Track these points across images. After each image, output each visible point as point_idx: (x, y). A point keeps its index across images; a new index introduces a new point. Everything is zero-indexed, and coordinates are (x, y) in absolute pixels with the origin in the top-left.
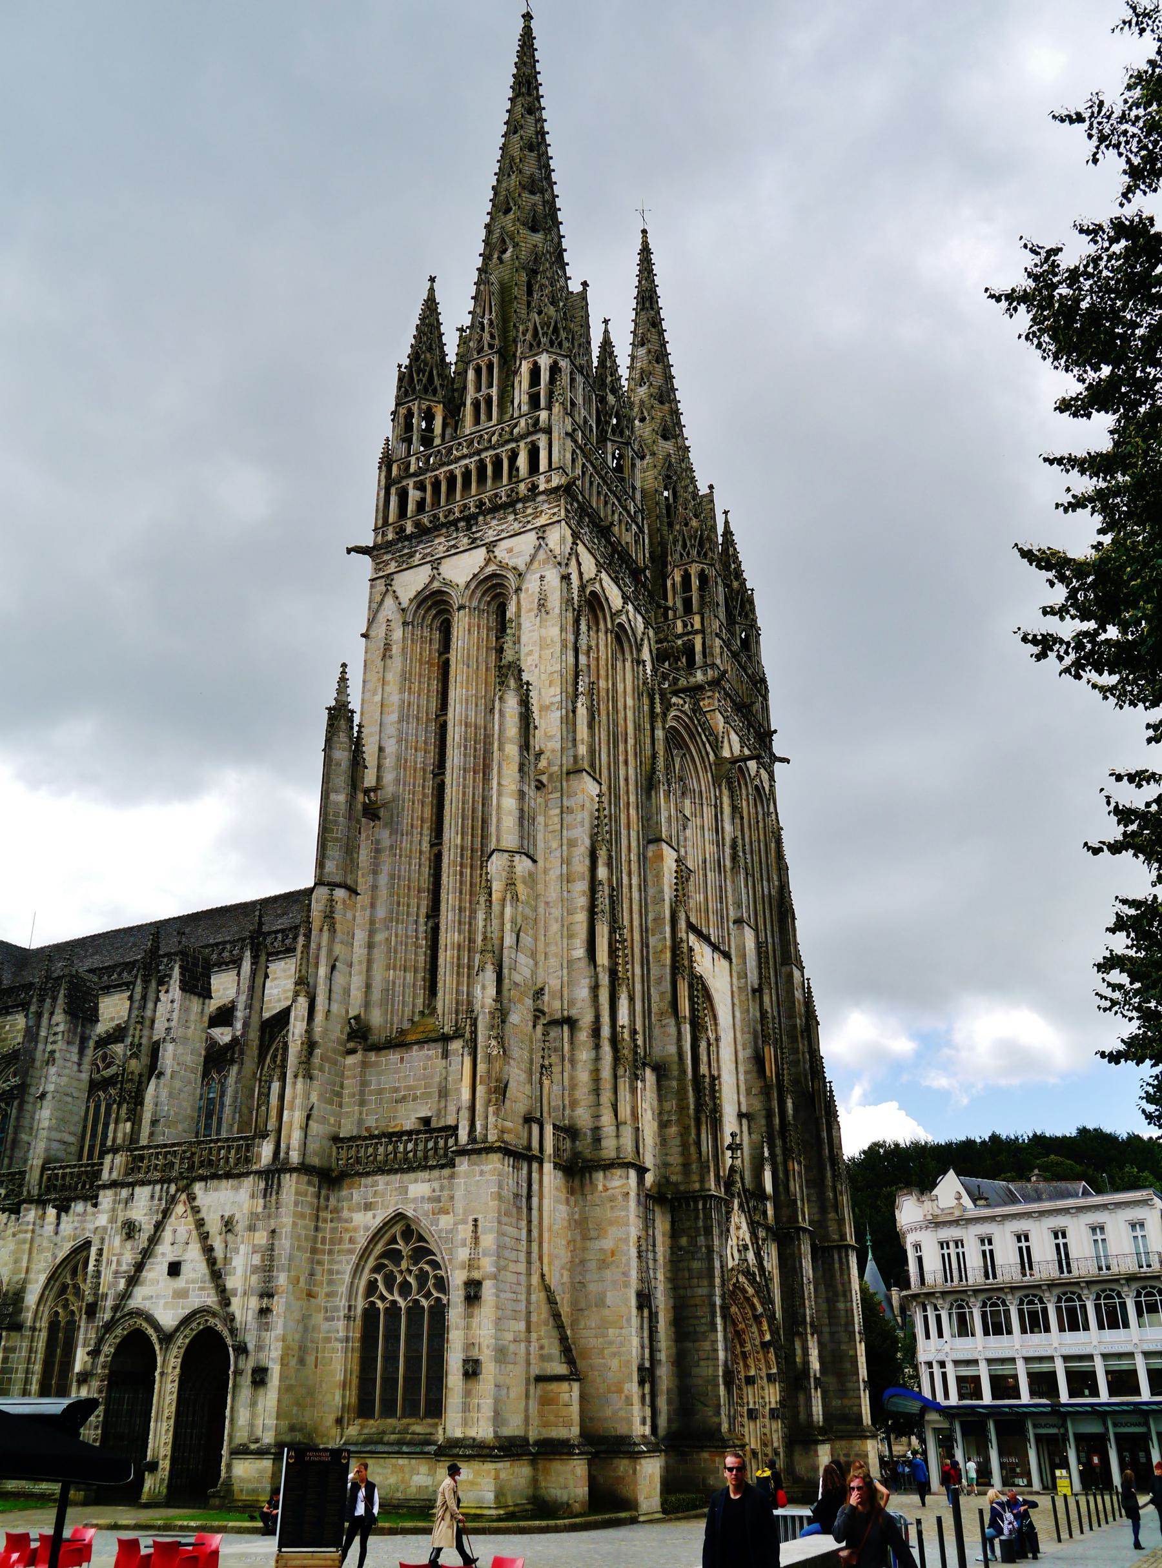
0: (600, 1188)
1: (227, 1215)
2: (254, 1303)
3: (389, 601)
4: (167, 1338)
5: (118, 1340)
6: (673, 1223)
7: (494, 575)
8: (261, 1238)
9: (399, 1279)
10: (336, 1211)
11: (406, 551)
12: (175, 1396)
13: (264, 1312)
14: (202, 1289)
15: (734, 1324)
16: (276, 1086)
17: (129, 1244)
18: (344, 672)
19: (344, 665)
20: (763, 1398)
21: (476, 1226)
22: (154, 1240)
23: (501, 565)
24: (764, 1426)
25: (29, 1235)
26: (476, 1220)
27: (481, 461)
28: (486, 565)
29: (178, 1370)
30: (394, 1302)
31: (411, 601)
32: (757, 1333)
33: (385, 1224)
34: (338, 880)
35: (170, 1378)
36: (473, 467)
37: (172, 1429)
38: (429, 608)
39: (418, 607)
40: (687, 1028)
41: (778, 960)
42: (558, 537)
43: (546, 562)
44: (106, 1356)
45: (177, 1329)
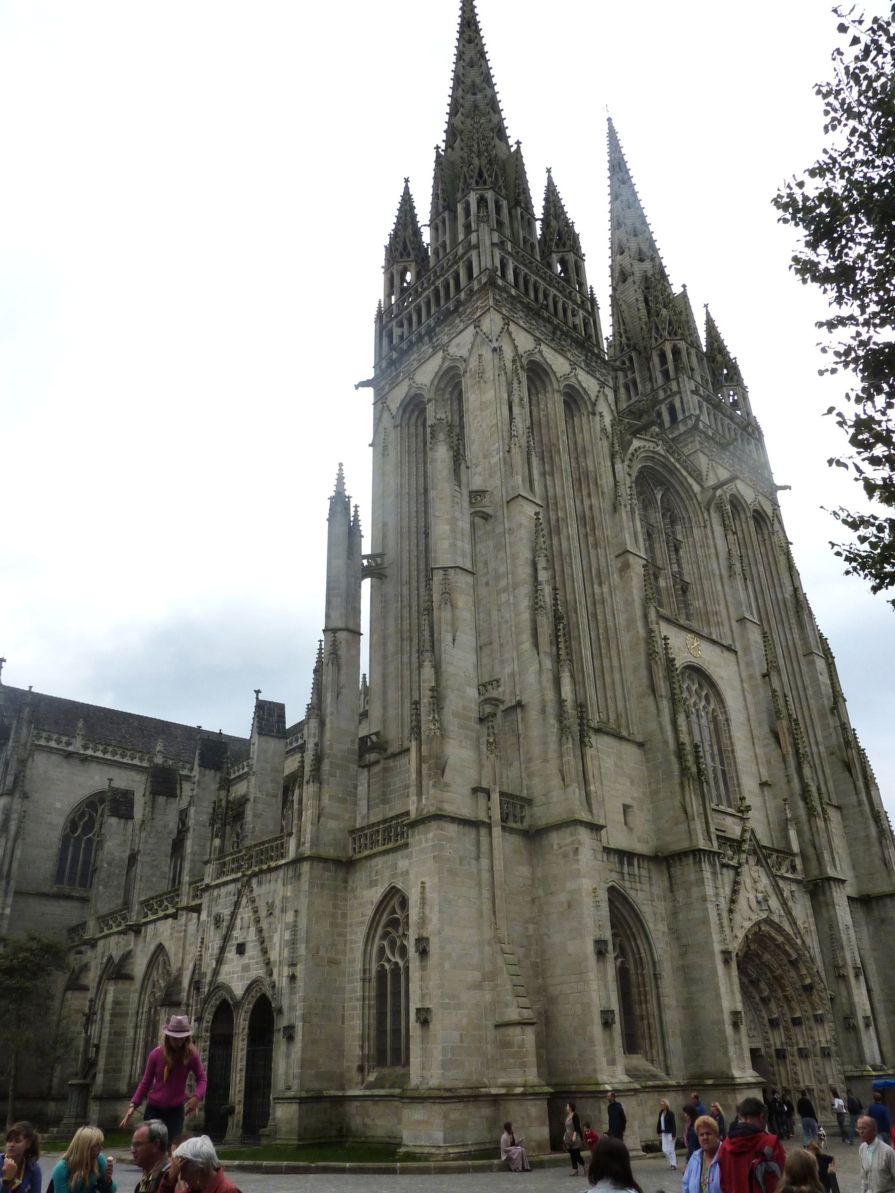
0: (556, 847)
1: (270, 901)
2: (286, 971)
3: (386, 415)
4: (238, 1004)
5: (214, 1009)
6: (670, 878)
7: (451, 368)
8: (289, 917)
9: (398, 944)
10: (353, 890)
11: (394, 374)
12: (245, 1052)
13: (293, 978)
14: (257, 963)
15: (772, 971)
16: (297, 792)
17: (219, 931)
18: (341, 470)
19: (341, 465)
20: (812, 1038)
21: (423, 888)
22: (231, 927)
23: (454, 360)
24: (817, 1064)
25: (183, 934)
26: (423, 883)
27: (437, 290)
28: (443, 363)
29: (246, 1030)
30: (396, 963)
31: (398, 409)
32: (795, 976)
33: (385, 897)
34: (341, 624)
35: (241, 1038)
36: (431, 296)
37: (244, 1079)
38: (413, 411)
39: (404, 412)
40: (665, 704)
41: (800, 652)
42: (492, 322)
43: (482, 343)
44: (208, 1022)
45: (243, 998)
